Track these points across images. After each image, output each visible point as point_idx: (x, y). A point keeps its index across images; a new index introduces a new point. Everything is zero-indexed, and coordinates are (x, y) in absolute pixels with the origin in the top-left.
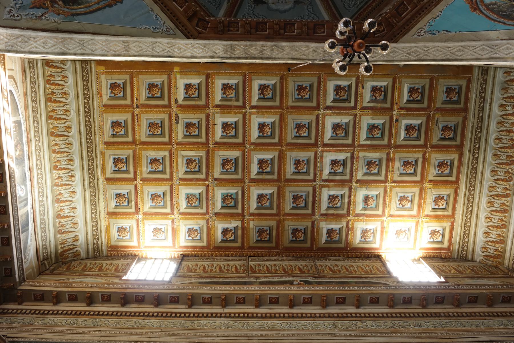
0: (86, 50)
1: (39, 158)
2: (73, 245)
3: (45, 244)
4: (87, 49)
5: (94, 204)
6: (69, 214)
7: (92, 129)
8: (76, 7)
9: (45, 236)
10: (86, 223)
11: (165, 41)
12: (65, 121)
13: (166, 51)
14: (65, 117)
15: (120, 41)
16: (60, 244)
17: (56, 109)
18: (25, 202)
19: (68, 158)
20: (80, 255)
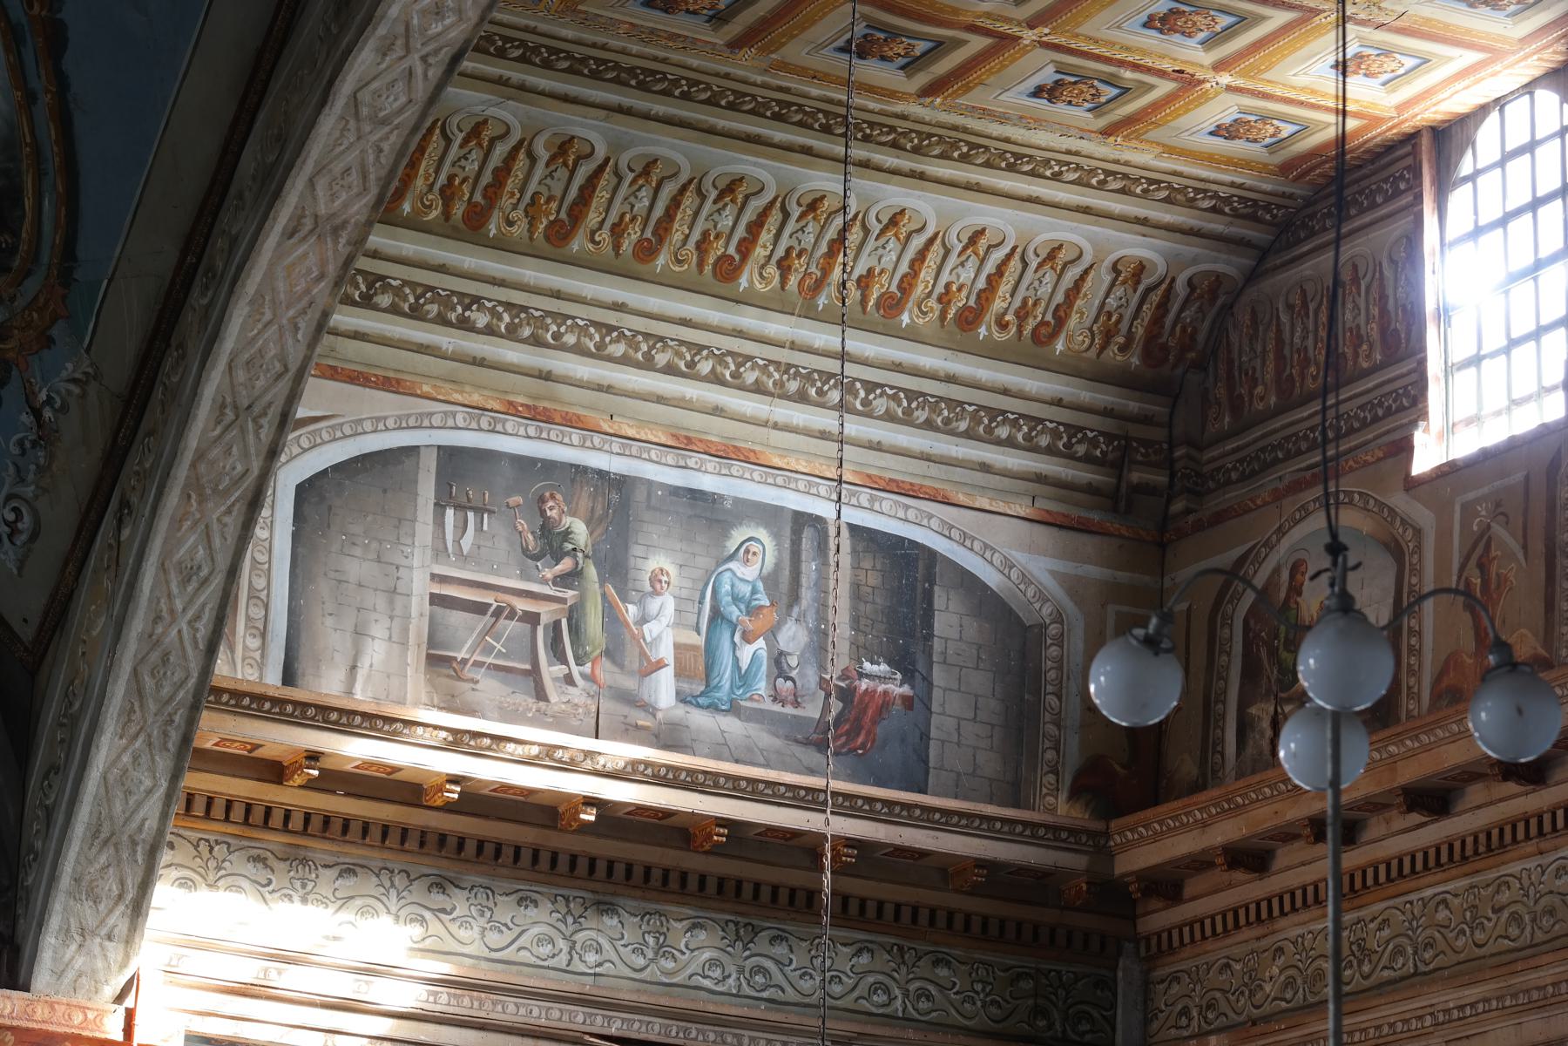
0: (270, 404)
1: (644, 347)
2: (1149, 290)
3: (1056, 435)
4: (268, 398)
5: (1015, 161)
6: (990, 267)
7: (626, 61)
8: (26, 226)
9: (1015, 424)
10: (1086, 210)
11: (364, 60)
12: (522, 155)
13: (419, 69)
14: (501, 150)
15: (279, 244)
16: (1103, 348)
17: (443, 178)
18: (808, 537)
19: (713, 194)
20: (1219, 278)
